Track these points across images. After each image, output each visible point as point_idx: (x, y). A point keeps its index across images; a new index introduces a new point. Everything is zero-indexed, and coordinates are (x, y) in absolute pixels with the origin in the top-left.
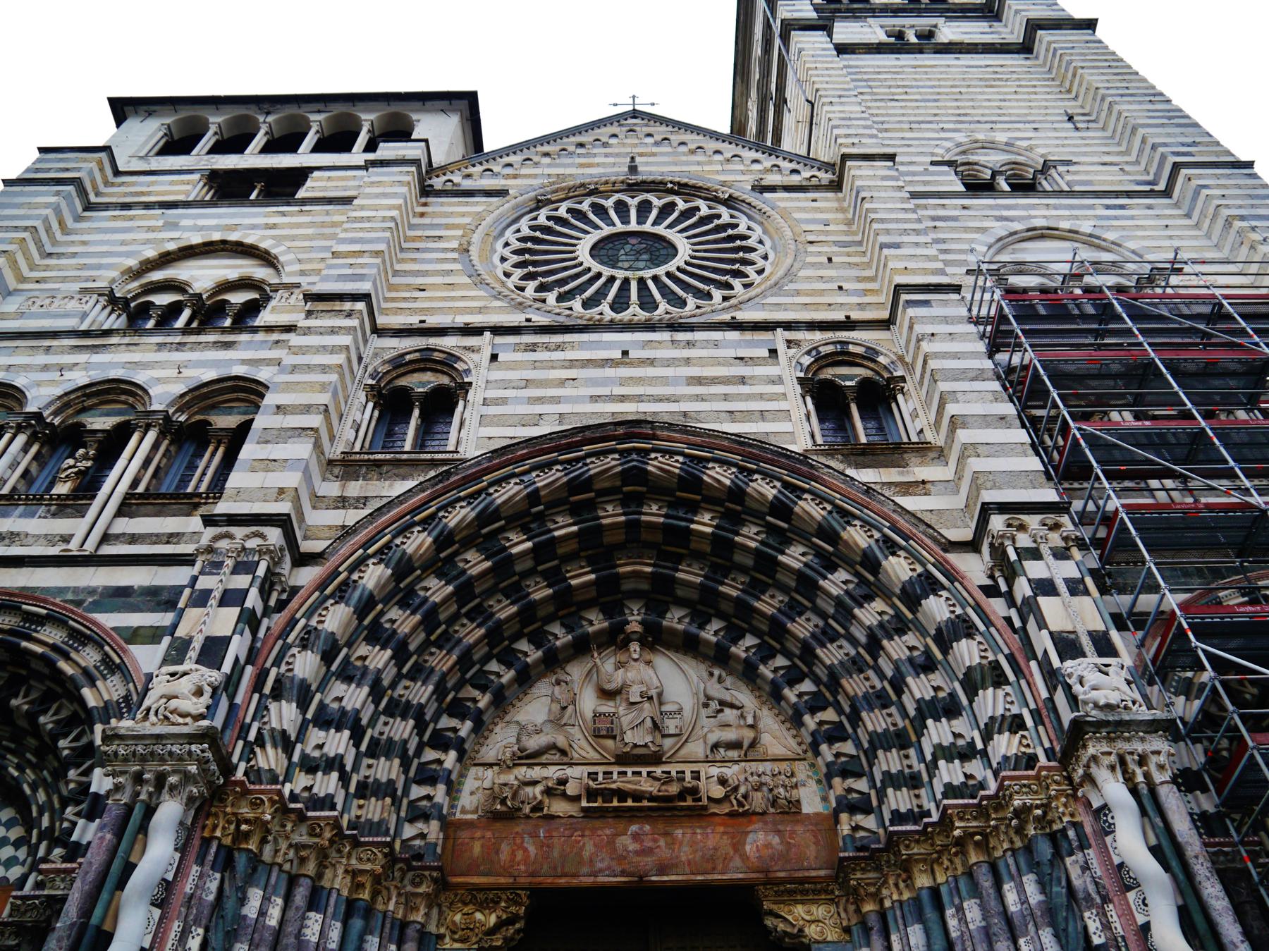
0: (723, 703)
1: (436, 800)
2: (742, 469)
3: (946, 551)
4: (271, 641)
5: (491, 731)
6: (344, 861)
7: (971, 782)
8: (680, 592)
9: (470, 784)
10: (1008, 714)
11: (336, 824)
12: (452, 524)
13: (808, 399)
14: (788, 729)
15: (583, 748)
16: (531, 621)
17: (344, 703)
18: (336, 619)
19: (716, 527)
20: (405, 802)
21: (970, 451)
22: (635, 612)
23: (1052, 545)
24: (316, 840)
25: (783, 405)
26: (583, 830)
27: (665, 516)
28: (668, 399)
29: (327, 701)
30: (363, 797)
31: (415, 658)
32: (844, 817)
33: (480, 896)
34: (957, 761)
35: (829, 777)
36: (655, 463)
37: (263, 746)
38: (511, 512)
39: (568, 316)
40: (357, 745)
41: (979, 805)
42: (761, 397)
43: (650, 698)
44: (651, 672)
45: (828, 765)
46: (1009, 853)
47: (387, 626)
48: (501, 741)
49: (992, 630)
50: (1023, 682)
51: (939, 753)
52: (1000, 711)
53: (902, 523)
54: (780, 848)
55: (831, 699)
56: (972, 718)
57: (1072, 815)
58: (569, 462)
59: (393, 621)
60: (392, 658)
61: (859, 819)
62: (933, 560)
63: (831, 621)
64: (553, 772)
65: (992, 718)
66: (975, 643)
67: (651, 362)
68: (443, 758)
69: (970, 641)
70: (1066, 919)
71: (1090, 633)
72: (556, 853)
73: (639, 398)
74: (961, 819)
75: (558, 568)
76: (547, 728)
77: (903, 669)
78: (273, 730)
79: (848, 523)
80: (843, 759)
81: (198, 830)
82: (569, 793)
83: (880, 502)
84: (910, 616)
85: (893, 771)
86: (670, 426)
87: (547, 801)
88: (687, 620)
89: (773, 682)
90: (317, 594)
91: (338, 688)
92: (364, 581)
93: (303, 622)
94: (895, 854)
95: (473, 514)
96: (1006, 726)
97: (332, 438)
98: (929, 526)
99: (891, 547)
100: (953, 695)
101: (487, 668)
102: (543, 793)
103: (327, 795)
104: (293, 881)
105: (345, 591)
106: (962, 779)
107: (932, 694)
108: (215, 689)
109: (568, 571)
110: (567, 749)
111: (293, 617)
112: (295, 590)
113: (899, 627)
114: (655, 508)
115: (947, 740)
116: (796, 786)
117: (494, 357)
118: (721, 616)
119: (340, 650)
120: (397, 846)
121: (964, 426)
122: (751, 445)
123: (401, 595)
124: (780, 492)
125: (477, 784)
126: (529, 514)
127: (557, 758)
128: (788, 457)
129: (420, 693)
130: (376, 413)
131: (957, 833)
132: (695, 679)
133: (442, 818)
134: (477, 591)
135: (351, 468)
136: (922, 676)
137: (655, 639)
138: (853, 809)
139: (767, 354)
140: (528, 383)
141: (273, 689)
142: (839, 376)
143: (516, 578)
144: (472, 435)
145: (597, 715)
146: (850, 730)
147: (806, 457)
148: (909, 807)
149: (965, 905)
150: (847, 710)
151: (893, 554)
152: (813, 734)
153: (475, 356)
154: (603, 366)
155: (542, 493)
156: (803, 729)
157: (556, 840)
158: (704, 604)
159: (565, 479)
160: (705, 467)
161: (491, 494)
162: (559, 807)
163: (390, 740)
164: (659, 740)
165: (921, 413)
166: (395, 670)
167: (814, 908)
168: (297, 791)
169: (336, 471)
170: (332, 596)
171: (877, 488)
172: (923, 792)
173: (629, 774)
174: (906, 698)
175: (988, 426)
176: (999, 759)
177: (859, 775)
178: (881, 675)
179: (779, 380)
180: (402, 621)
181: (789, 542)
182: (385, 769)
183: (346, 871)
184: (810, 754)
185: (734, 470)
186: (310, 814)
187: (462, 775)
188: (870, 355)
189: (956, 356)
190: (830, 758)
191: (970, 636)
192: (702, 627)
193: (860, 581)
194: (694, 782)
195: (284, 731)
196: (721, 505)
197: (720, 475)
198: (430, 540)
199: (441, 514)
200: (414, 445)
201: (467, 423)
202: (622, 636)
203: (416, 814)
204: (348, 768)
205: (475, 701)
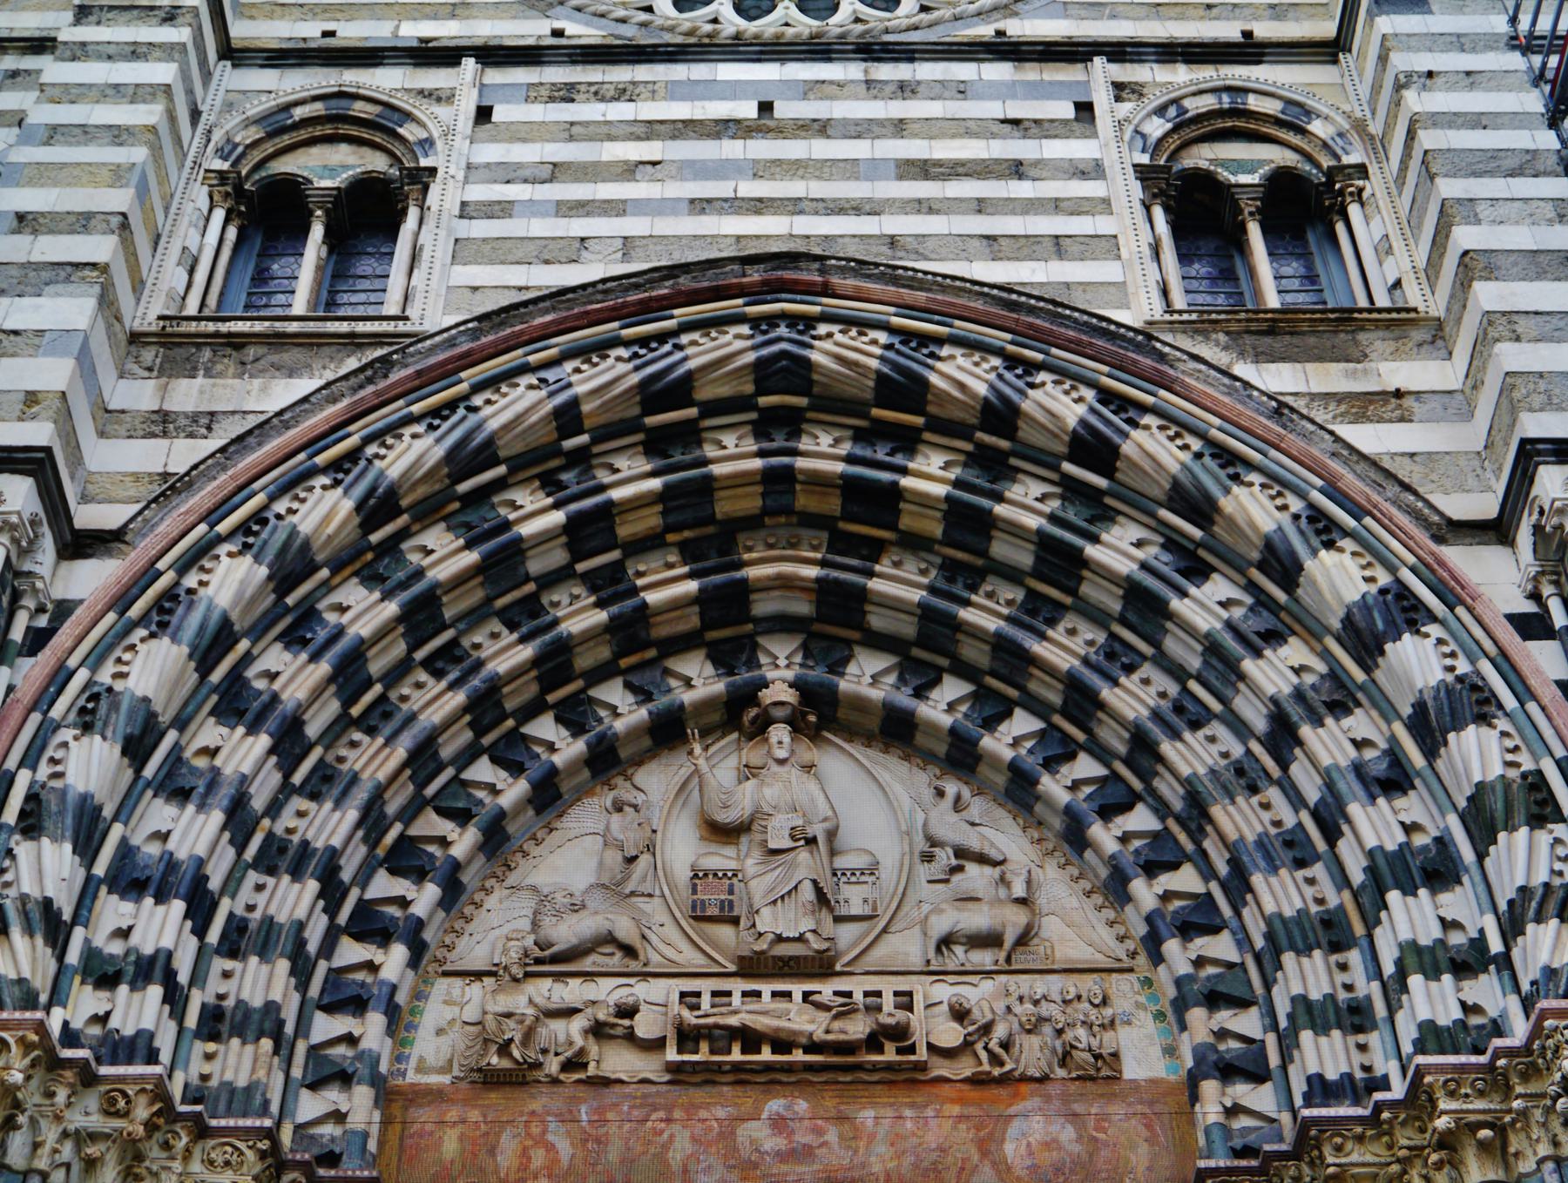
0: (961, 853)
1: (365, 1044)
2: (1012, 361)
3: (1439, 539)
4: (17, 714)
5: (478, 906)
6: (177, 1166)
7: (1475, 1020)
8: (878, 621)
9: (434, 1013)
10: (1557, 881)
11: (159, 1093)
12: (394, 473)
13: (1158, 213)
14: (1099, 909)
15: (670, 942)
17: (171, 845)
18: (154, 669)
19: (958, 484)
21: (1501, 328)
22: (782, 662)
24: (118, 1123)
25: (1102, 225)
26: (670, 1109)
27: (850, 459)
28: (856, 208)
29: (136, 840)
30: (214, 1037)
31: (317, 752)
32: (1209, 1087)
34: (1447, 978)
35: (1181, 1006)
36: (827, 345)
38: (519, 448)
39: (644, 25)
40: (200, 932)
41: (1491, 1067)
42: (1057, 206)
43: (811, 841)
44: (812, 786)
45: (1179, 982)
46: (1550, 1165)
47: (260, 684)
48: (497, 926)
49: (1532, 707)
51: (1411, 961)
52: (1541, 876)
53: (1350, 481)
54: (1076, 1148)
55: (1189, 847)
56: (1481, 888)
58: (643, 341)
59: (272, 676)
60: (271, 751)
61: (1242, 1092)
62: (1411, 559)
63: (1193, 686)
64: (608, 992)
65: (1523, 890)
66: (1495, 734)
67: (822, 128)
69: (1484, 730)
72: (613, 1154)
73: (794, 206)
74: (1452, 1094)
75: (618, 566)
76: (595, 901)
77: (1342, 786)
78: (24, 898)
79: (1235, 478)
80: (1211, 970)
82: (641, 1032)
84: (1359, 675)
85: (1315, 995)
86: (861, 267)
88: (891, 679)
89: (1068, 811)
90: (111, 617)
91: (159, 813)
92: (209, 591)
93: (82, 675)
94: (1312, 1164)
95: (439, 452)
96: (1552, 906)
97: (138, 286)
98: (1407, 487)
99: (1325, 531)
100: (1443, 842)
101: (469, 774)
102: (586, 1032)
103: (139, 1033)
105: (170, 612)
106: (1457, 1014)
107: (1401, 837)
109: (640, 574)
110: (637, 943)
111: (61, 665)
112: (64, 609)
113: (1339, 699)
114: (825, 441)
115: (1429, 933)
117: (483, 114)
118: (963, 670)
119: (163, 734)
120: (286, 1136)
121: (1491, 273)
122: (1032, 310)
123: (288, 620)
124: (1092, 410)
125: (450, 1013)
126: (559, 453)
127: (616, 961)
128: (1112, 336)
129: (329, 825)
130: (232, 233)
131: (1442, 1123)
132: (906, 802)
133: (377, 1081)
134: (448, 614)
135: (180, 353)
136: (1381, 801)
137: (820, 714)
138: (1228, 1072)
139: (1068, 111)
140: (557, 171)
141: (23, 814)
142: (1223, 163)
143: (530, 587)
144: (435, 282)
145: (698, 875)
146: (1227, 911)
147: (1150, 337)
148: (1345, 1069)
150: (1223, 869)
151: (1329, 545)
152: (1149, 919)
153: (442, 111)
154: (717, 136)
155: (586, 408)
156: (1129, 909)
157: (613, 1129)
158: (929, 647)
159: (635, 378)
160: (932, 355)
161: (475, 409)
162: (618, 1061)
163: (269, 922)
164: (828, 927)
165: (1397, 244)
166: (277, 777)
168: (77, 1024)
169: (148, 355)
171: (1300, 404)
172: (1373, 1039)
173: (766, 996)
174: (1345, 847)
175: (1540, 275)
176: (1534, 973)
177: (1243, 1003)
178: (1296, 798)
179: (1093, 170)
180: (292, 676)
181: (1107, 516)
182: (260, 982)
184: (1142, 960)
185: (996, 362)
186: (104, 1070)
187: (418, 995)
188: (1294, 118)
189: (1478, 121)
190: (1184, 969)
191: (1483, 719)
192: (920, 693)
193: (1259, 602)
194: (901, 1015)
195: (47, 903)
196: (969, 438)
197: (963, 375)
198: (348, 505)
199: (371, 450)
200: (313, 303)
201: (426, 255)
202: (753, 712)
203: (328, 1073)
204: (183, 978)
205: (444, 842)
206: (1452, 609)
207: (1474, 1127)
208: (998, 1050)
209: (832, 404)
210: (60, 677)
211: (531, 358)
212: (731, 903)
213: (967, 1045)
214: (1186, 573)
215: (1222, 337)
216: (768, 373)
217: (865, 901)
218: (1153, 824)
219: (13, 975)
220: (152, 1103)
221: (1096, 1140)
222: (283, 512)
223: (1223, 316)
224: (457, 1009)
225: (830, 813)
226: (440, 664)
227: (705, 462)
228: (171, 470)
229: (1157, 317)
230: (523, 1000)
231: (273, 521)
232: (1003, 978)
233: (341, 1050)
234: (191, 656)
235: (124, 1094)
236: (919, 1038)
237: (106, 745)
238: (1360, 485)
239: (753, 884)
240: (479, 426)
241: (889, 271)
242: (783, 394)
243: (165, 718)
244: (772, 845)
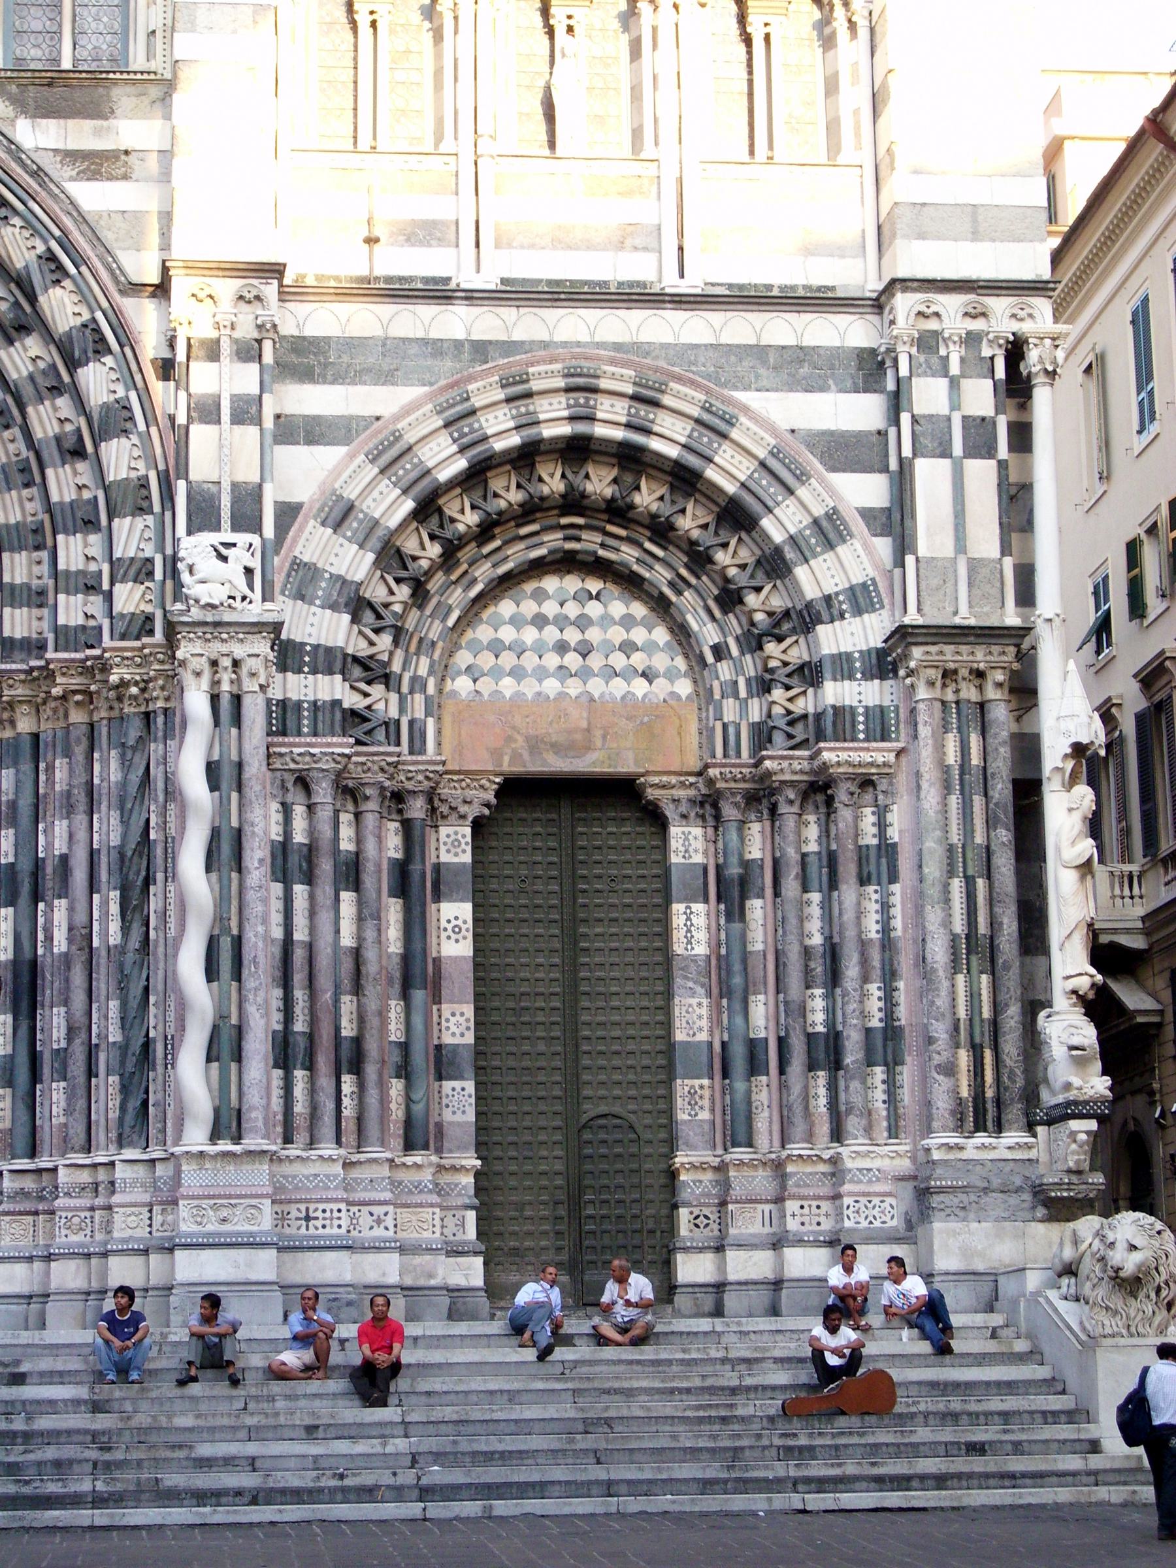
10: (141, 555)
23: (237, 334)
46: (105, 722)
49: (153, 430)
50: (168, 514)
57: (167, 699)
69: (123, 440)
70: (131, 810)
71: (235, 485)
74: (64, 674)
131: (56, 691)
149: (57, 763)
206: (121, 346)
207: (75, 692)
215: (14, 88)
223: (15, 74)
238: (81, 240)
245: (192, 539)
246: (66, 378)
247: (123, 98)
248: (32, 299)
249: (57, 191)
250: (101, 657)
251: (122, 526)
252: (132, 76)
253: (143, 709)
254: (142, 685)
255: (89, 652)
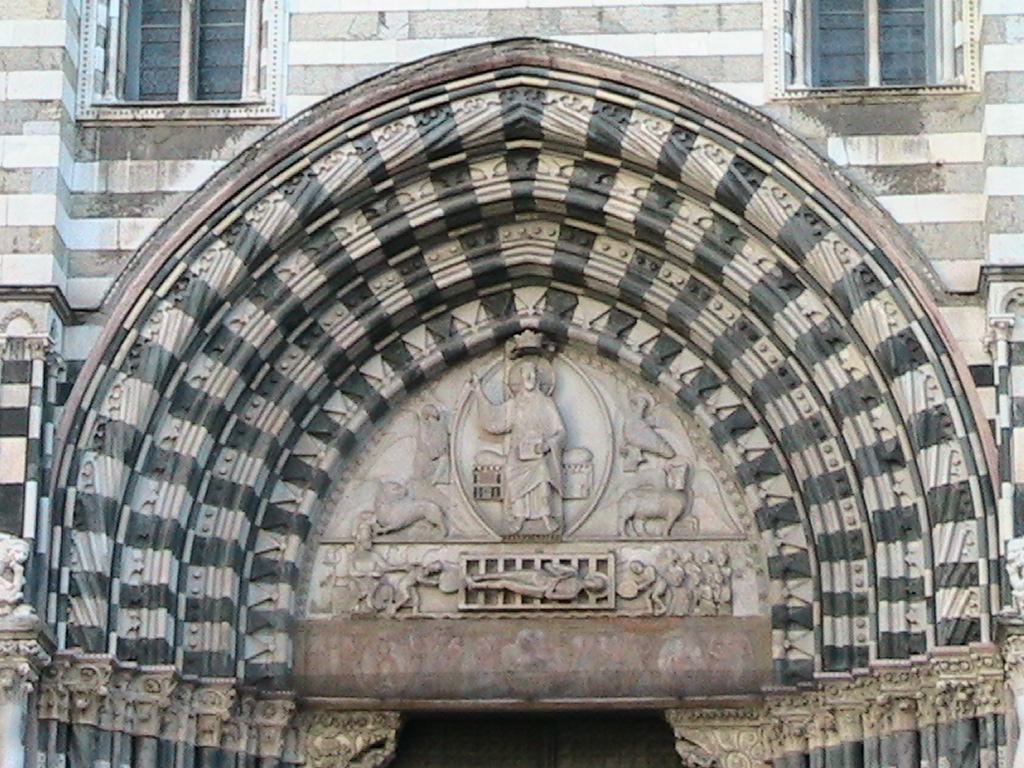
2: (679, 129)
5: (341, 492)
9: (319, 572)
15: (464, 518)
16: (384, 335)
20: (243, 611)
21: (996, 155)
22: (531, 311)
29: (137, 509)
32: (778, 633)
33: (343, 717)
37: (77, 594)
46: (932, 729)
47: (195, 385)
50: (991, 519)
52: (954, 559)
61: (795, 633)
64: (427, 555)
68: (283, 546)
78: (87, 574)
81: (34, 713)
83: (867, 212)
87: (416, 599)
88: (604, 322)
90: (103, 368)
95: (294, 214)
99: (869, 284)
104: (136, 741)
108: (24, 564)
112: (74, 368)
116: (726, 581)
123: (208, 340)
124: (730, 172)
129: (246, 469)
151: (872, 294)
161: (315, 176)
167: (734, 735)
170: (122, 369)
173: (519, 564)
183: (190, 717)
184: (754, 531)
186: (145, 668)
187: (308, 558)
198: (238, 262)
199: (249, 216)
208: (657, 600)
209: (560, 146)
210: (80, 417)
211: (351, 134)
212: (498, 489)
213: (641, 592)
214: (786, 288)
216: (512, 131)
217: (583, 487)
218: (766, 444)
219: (89, 624)
220: (172, 683)
221: (712, 656)
222: (197, 273)
224: (331, 568)
225: (561, 427)
226: (305, 342)
227: (472, 189)
228: (123, 247)
229: (780, 96)
230: (371, 565)
231: (192, 280)
232: (666, 545)
233: (266, 607)
234: (155, 387)
235: (156, 681)
236: (610, 592)
237: (115, 461)
239: (510, 484)
240: (320, 188)
241: (595, 54)
242: (520, 140)
243: (143, 430)
244: (522, 457)
245: (1018, 541)
246: (882, 388)
247: (933, 116)
248: (848, 313)
249: (869, 205)
250: (927, 662)
251: (944, 532)
252: (941, 91)
253: (971, 714)
254: (969, 691)
255: (914, 658)
